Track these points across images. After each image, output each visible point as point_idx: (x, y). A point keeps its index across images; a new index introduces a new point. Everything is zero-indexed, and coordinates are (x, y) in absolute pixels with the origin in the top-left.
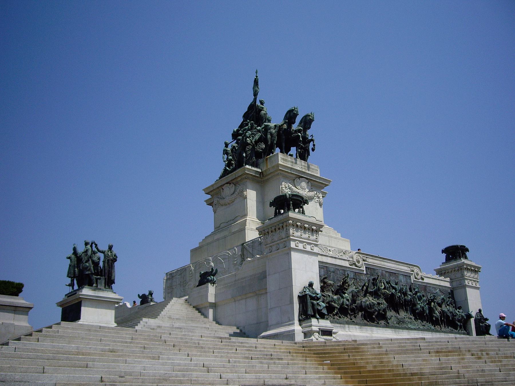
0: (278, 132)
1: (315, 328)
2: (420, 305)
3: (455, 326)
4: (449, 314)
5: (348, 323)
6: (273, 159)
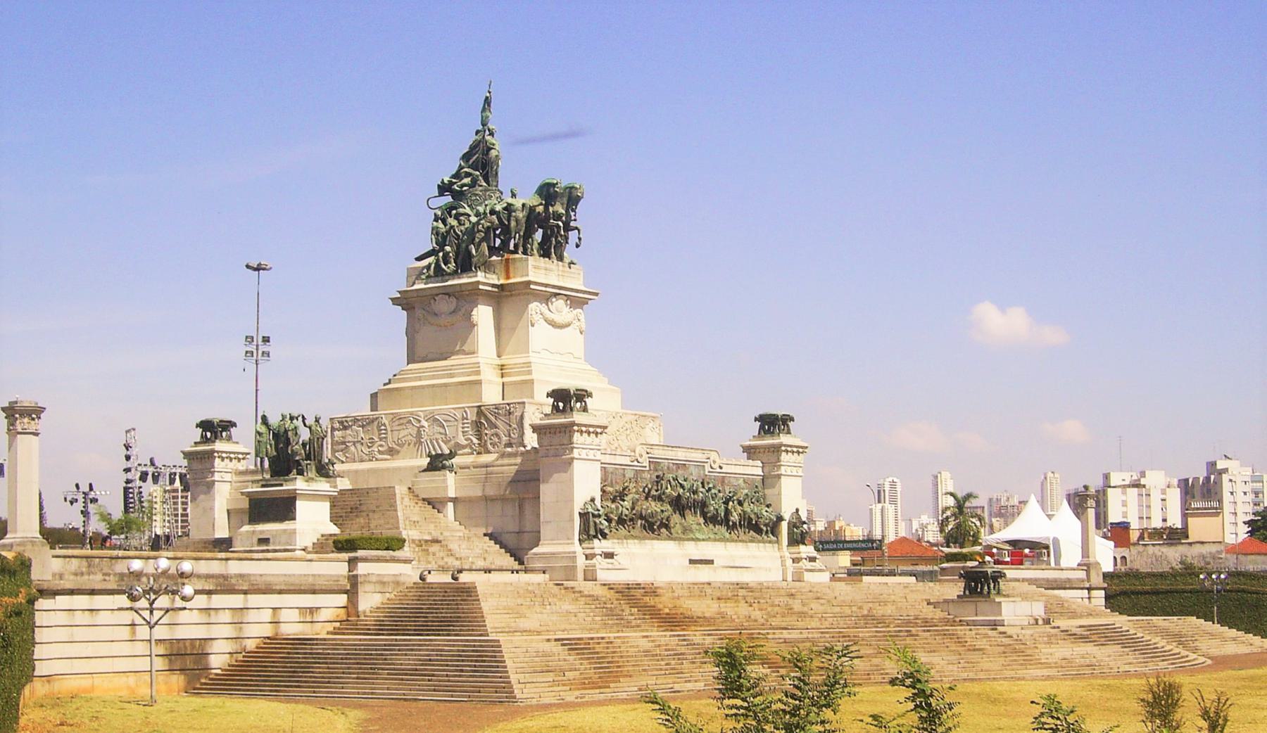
0: (528, 218)
1: (598, 551)
2: (715, 506)
3: (759, 531)
4: (753, 516)
5: (626, 538)
6: (518, 264)
